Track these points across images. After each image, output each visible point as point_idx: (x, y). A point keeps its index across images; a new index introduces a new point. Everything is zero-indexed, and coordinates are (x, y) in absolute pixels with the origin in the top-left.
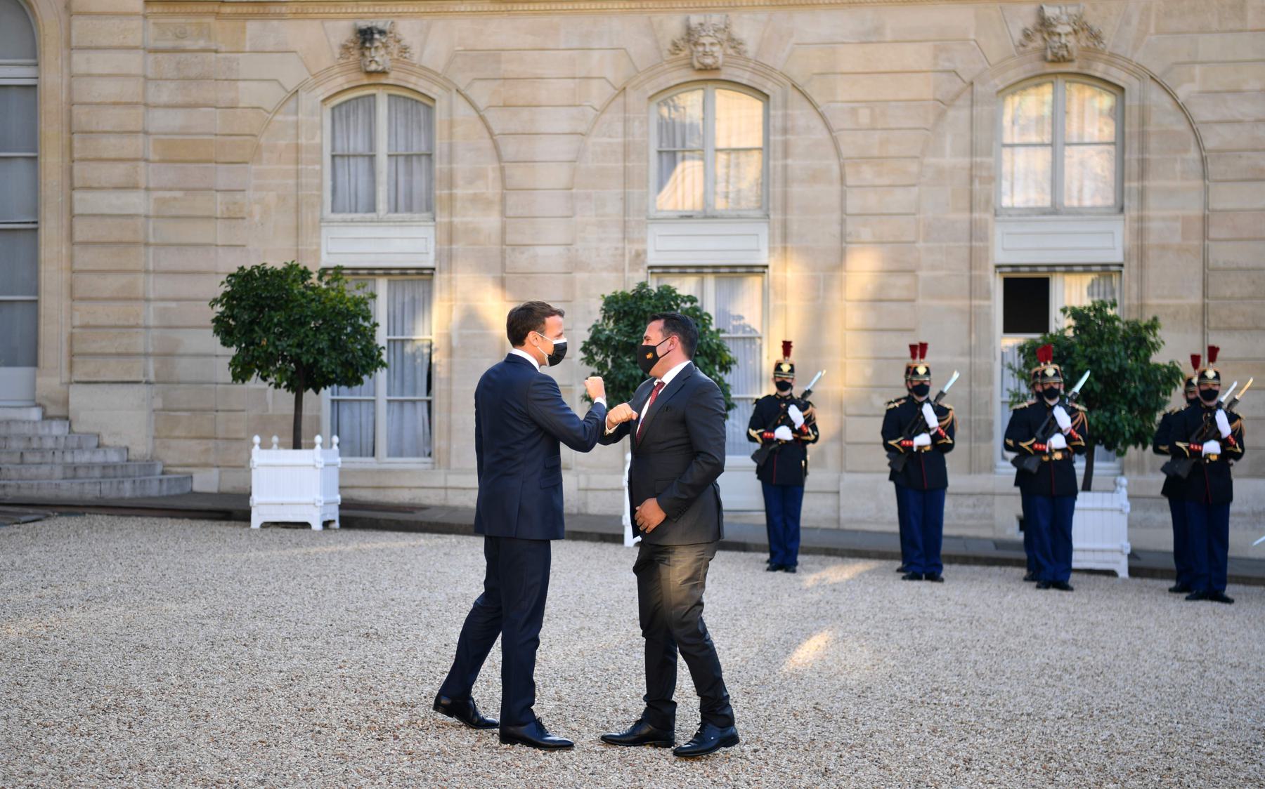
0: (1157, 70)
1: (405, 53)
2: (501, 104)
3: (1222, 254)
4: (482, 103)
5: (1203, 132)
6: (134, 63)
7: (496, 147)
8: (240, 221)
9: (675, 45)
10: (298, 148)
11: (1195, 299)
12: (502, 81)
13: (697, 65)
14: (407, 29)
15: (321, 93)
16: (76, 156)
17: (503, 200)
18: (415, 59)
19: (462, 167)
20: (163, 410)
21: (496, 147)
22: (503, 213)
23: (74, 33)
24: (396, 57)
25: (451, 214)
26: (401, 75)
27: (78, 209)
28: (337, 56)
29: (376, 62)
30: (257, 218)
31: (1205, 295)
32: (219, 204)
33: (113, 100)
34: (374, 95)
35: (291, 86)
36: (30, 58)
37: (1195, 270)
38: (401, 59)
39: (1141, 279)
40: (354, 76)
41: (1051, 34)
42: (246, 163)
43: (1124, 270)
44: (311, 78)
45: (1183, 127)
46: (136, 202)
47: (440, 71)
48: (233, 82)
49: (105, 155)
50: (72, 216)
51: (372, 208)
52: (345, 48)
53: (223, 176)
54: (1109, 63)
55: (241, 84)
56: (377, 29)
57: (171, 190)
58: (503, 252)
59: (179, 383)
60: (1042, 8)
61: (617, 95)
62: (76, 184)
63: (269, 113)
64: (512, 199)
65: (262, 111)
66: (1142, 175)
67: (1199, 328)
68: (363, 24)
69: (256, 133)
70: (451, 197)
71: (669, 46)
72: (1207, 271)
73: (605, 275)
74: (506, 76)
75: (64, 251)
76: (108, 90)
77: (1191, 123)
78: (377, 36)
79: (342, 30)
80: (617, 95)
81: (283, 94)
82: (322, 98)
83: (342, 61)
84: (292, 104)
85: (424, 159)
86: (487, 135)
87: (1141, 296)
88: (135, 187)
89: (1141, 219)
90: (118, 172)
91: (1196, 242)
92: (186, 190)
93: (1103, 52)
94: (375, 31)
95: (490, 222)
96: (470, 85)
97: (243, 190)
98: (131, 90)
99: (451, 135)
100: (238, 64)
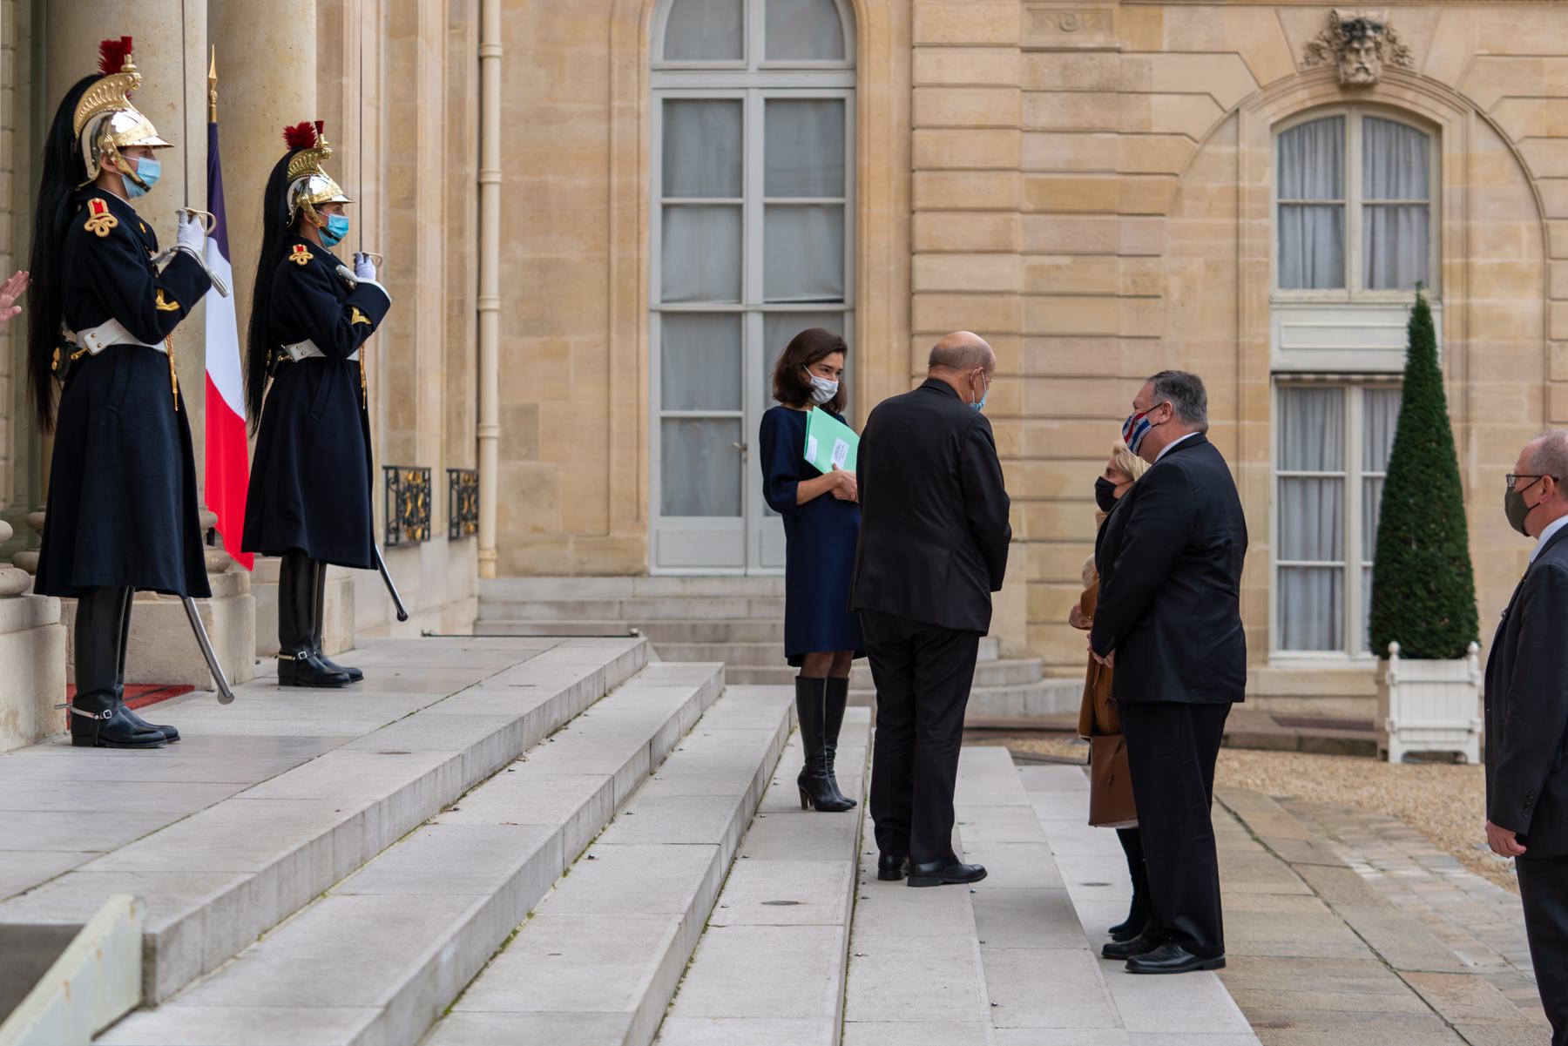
1: (1402, 57)
2: (1544, 134)
4: (1514, 131)
6: (1009, 66)
7: (1535, 195)
8: (1153, 301)
10: (1238, 193)
12: (1544, 101)
14: (1404, 23)
15: (1273, 112)
16: (919, 204)
17: (1546, 273)
18: (1417, 67)
19: (1482, 226)
20: (1040, 582)
21: (1535, 195)
22: (1546, 293)
23: (918, 24)
24: (1388, 62)
25: (1468, 294)
26: (1393, 89)
27: (921, 283)
28: (1300, 59)
29: (1366, 70)
30: (1175, 297)
32: (1119, 275)
33: (975, 122)
34: (1343, 117)
35: (1229, 105)
38: (1396, 66)
40: (1320, 89)
42: (1163, 215)
44: (1259, 91)
46: (1010, 272)
47: (1452, 84)
48: (1142, 96)
49: (963, 204)
50: (911, 292)
51: (1339, 281)
52: (1315, 49)
53: (1129, 235)
55: (1154, 99)
56: (1370, 22)
57: (1051, 254)
59: (1063, 541)
62: (920, 245)
63: (1196, 142)
65: (1185, 138)
68: (1346, 15)
69: (1177, 172)
70: (1467, 269)
74: (1551, 95)
75: (895, 345)
76: (968, 107)
78: (1370, 33)
79: (1308, 24)
81: (1219, 114)
82: (1273, 120)
83: (1306, 68)
84: (1229, 129)
85: (1415, 215)
86: (1520, 178)
88: (1008, 252)
90: (981, 229)
92: (1076, 254)
94: (1368, 26)
95: (1526, 305)
96: (1496, 106)
97: (1158, 256)
98: (1000, 107)
99: (1467, 177)
100: (1151, 69)
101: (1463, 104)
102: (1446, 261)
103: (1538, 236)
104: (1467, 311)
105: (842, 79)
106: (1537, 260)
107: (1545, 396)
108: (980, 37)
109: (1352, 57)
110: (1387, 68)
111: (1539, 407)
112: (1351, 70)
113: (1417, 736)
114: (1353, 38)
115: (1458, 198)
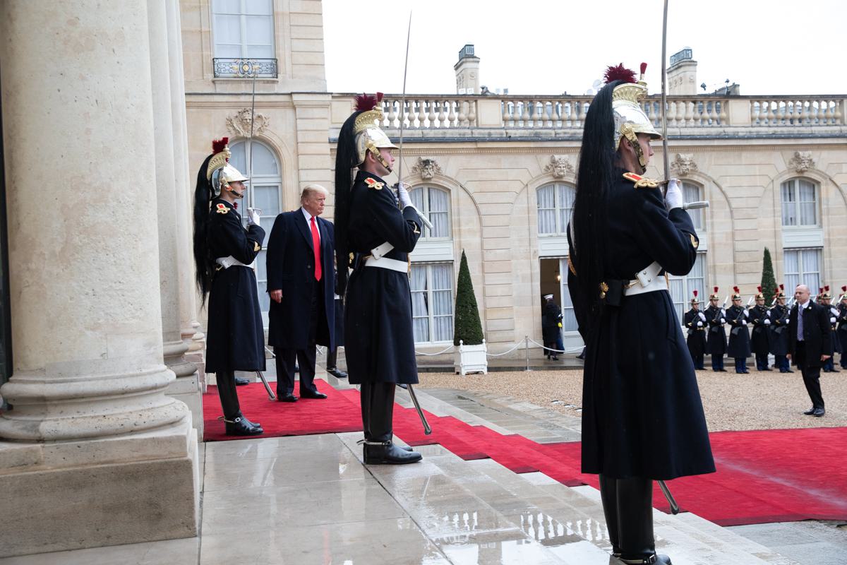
0: (715, 178)
3: (740, 246)
4: (471, 191)
5: (731, 200)
9: (547, 167)
11: (731, 263)
13: (557, 175)
14: (439, 160)
17: (481, 231)
22: (481, 236)
25: (460, 238)
31: (734, 261)
36: (274, 173)
37: (730, 252)
39: (714, 256)
41: (681, 165)
43: (707, 253)
45: (723, 199)
47: (453, 177)
52: (415, 168)
54: (699, 176)
58: (482, 253)
60: (678, 155)
61: (524, 188)
64: (485, 230)
66: (712, 217)
67: (733, 273)
68: (424, 158)
71: (544, 168)
72: (734, 251)
73: (522, 260)
77: (727, 198)
80: (524, 188)
86: (473, 204)
87: (714, 262)
89: (713, 234)
91: (730, 242)
93: (697, 171)
95: (477, 240)
99: (458, 204)
101: (456, 183)
102: (453, 228)
103: (478, 219)
104: (460, 242)
105: (278, 180)
106: (479, 227)
107: (483, 265)
108: (319, 167)
109: (426, 170)
110: (435, 173)
111: (481, 269)
112: (424, 174)
113: (469, 368)
114: (426, 165)
115: (456, 211)
